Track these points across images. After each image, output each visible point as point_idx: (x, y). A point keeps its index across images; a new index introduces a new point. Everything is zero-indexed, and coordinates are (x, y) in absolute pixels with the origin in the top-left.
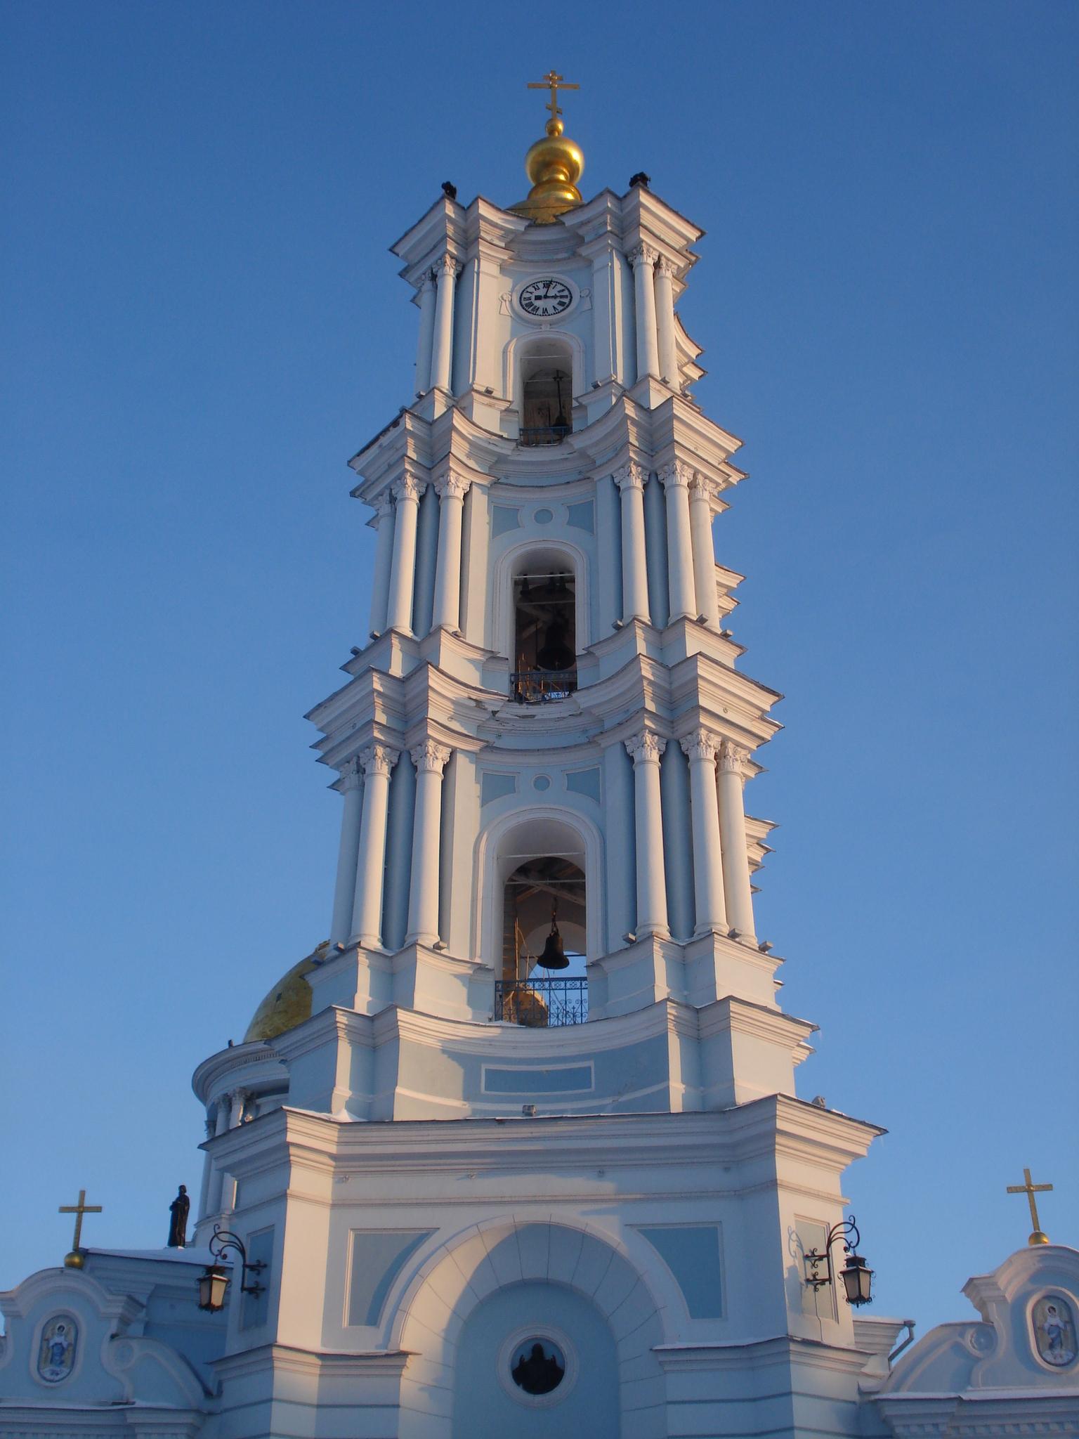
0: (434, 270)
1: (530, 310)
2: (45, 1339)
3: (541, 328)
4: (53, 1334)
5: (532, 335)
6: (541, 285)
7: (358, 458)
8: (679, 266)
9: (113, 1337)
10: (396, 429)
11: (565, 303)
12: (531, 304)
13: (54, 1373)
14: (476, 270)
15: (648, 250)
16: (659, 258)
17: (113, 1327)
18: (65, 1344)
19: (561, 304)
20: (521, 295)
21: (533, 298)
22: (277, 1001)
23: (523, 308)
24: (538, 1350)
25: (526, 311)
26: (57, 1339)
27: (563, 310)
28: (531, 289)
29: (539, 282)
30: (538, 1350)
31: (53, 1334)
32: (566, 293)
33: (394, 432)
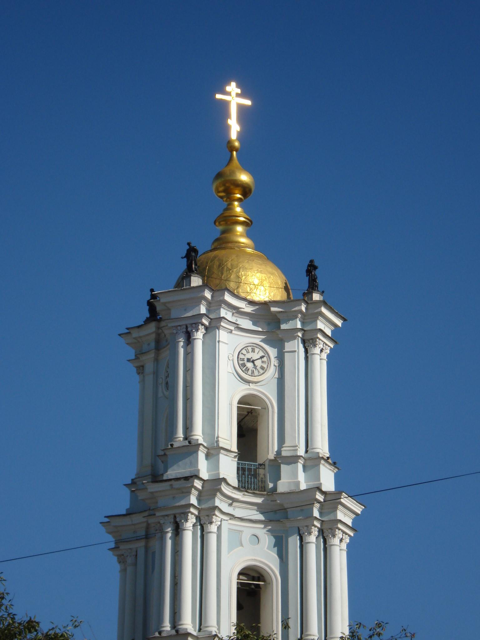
0: (189, 329)
1: (244, 369)
3: (249, 385)
5: (242, 390)
6: (250, 349)
7: (151, 483)
10: (186, 481)
11: (265, 368)
12: (244, 365)
14: (217, 339)
19: (262, 368)
21: (246, 360)
23: (240, 367)
25: (242, 370)
27: (263, 373)
28: (244, 352)
33: (182, 481)
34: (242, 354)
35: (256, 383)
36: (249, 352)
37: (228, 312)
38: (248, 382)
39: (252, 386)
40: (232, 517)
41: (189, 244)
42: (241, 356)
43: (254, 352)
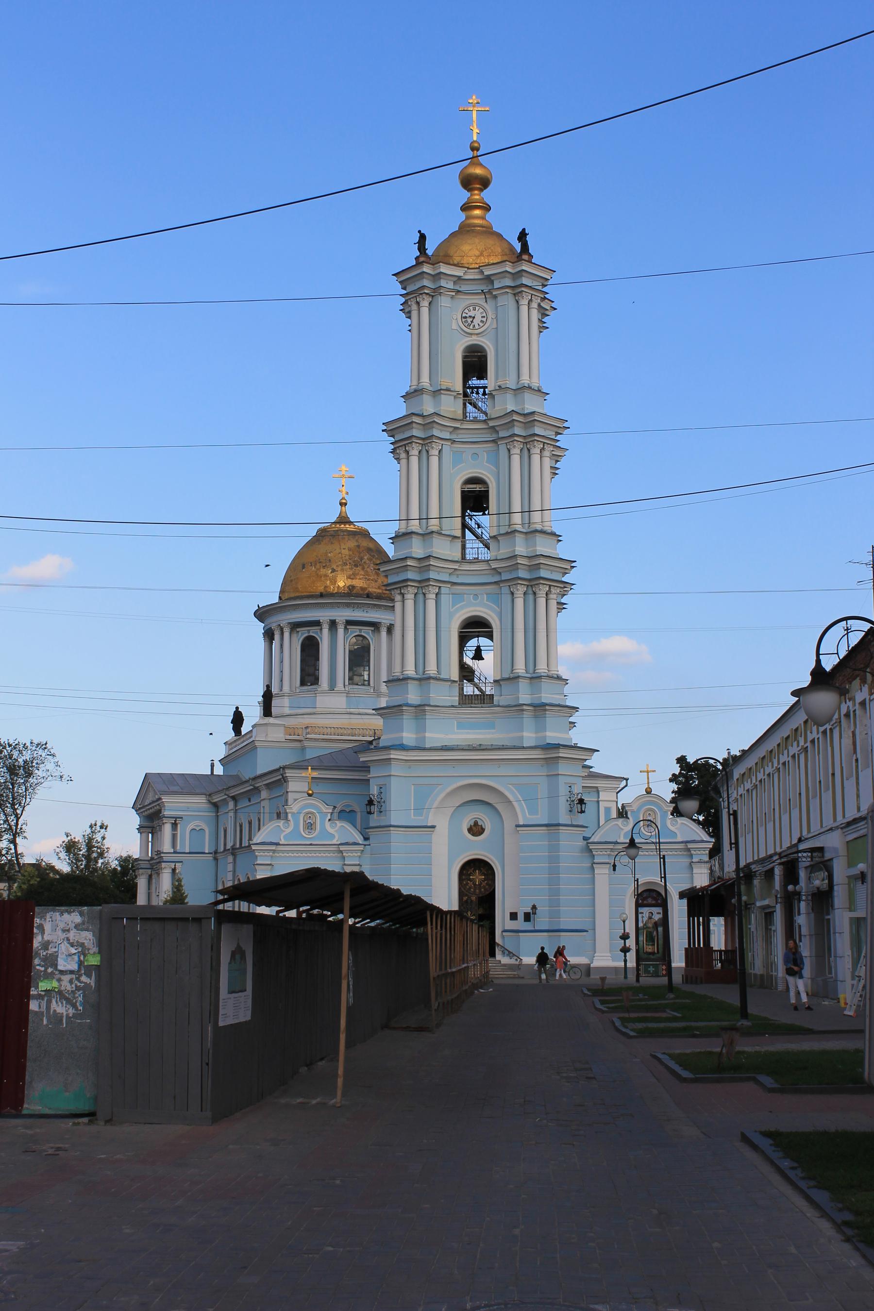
2: (304, 821)
4: (307, 819)
6: (471, 308)
8: (541, 297)
9: (329, 820)
12: (466, 321)
13: (309, 832)
15: (526, 295)
16: (531, 296)
17: (329, 817)
18: (312, 823)
19: (482, 321)
20: (462, 315)
22: (303, 569)
24: (476, 823)
26: (309, 821)
28: (466, 311)
29: (470, 306)
30: (476, 823)
31: (307, 819)
32: (484, 314)
34: (465, 313)
35: (477, 334)
36: (471, 311)
37: (448, 281)
38: (471, 334)
39: (474, 337)
40: (453, 442)
41: (419, 232)
42: (464, 315)
43: (475, 310)
